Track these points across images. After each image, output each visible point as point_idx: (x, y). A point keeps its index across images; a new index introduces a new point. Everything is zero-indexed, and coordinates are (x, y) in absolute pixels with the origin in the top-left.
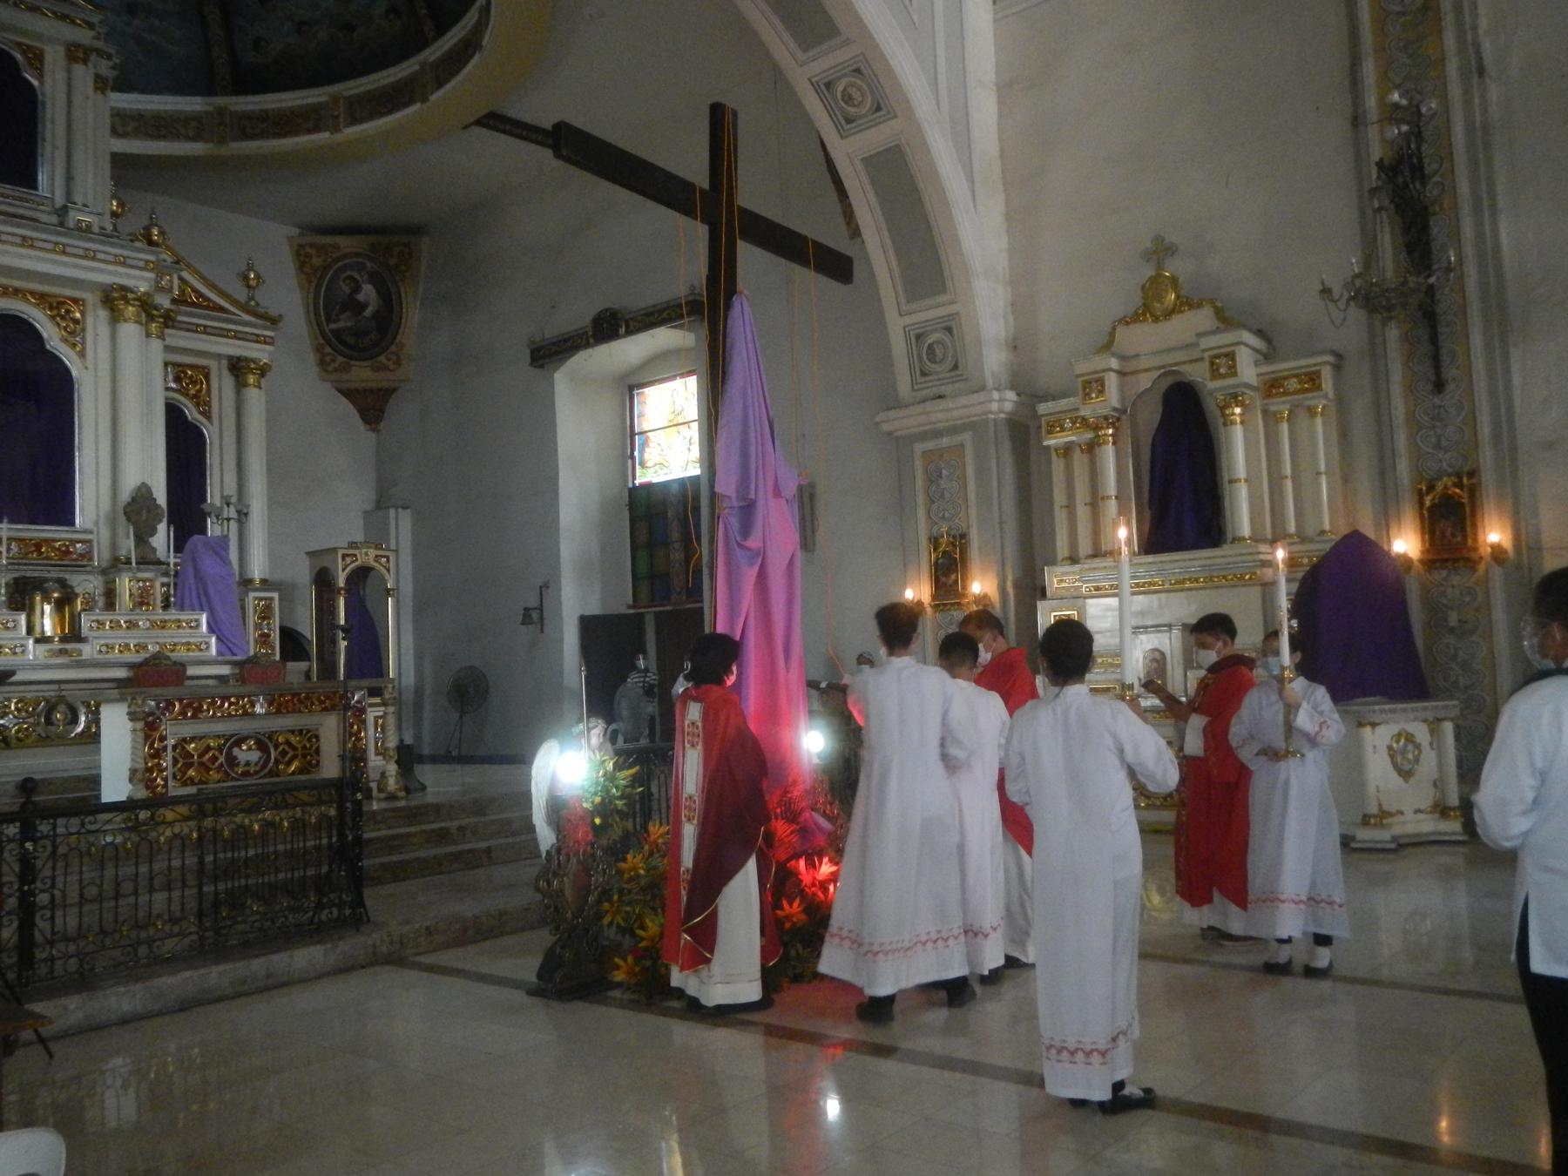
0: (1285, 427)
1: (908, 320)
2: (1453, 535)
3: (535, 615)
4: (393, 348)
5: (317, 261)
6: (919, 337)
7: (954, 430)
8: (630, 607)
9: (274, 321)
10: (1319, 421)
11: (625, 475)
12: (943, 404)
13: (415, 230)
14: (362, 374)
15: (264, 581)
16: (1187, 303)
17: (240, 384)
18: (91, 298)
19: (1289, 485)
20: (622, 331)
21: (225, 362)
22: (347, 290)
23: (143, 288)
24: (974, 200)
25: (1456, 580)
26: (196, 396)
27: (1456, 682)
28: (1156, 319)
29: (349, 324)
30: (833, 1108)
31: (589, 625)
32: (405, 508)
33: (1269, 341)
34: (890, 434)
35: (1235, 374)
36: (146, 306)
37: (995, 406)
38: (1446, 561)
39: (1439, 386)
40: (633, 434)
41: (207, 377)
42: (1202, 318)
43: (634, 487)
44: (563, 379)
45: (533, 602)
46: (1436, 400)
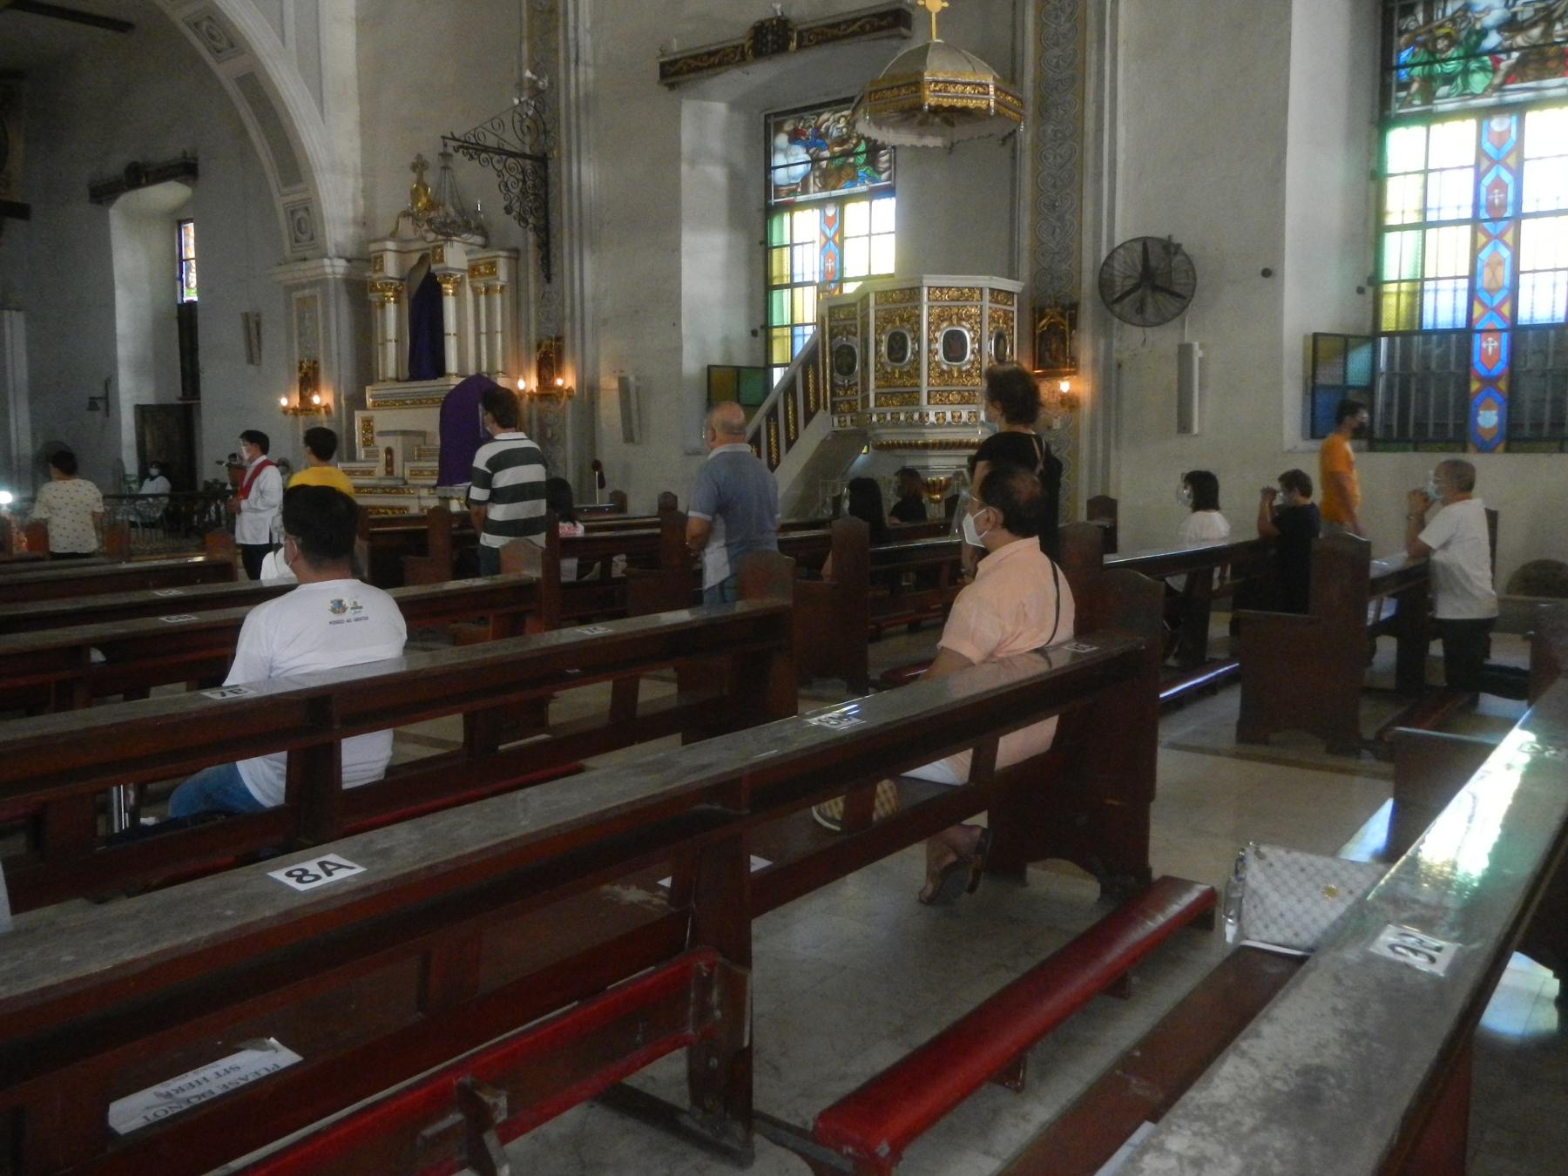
0: (483, 298)
3: (101, 404)
7: (313, 284)
10: (498, 297)
11: (175, 292)
12: (303, 266)
19: (483, 338)
24: (322, 112)
25: (552, 408)
31: (142, 412)
32: (18, 310)
33: (485, 234)
37: (328, 270)
39: (548, 278)
44: (116, 214)
45: (98, 391)
46: (548, 287)
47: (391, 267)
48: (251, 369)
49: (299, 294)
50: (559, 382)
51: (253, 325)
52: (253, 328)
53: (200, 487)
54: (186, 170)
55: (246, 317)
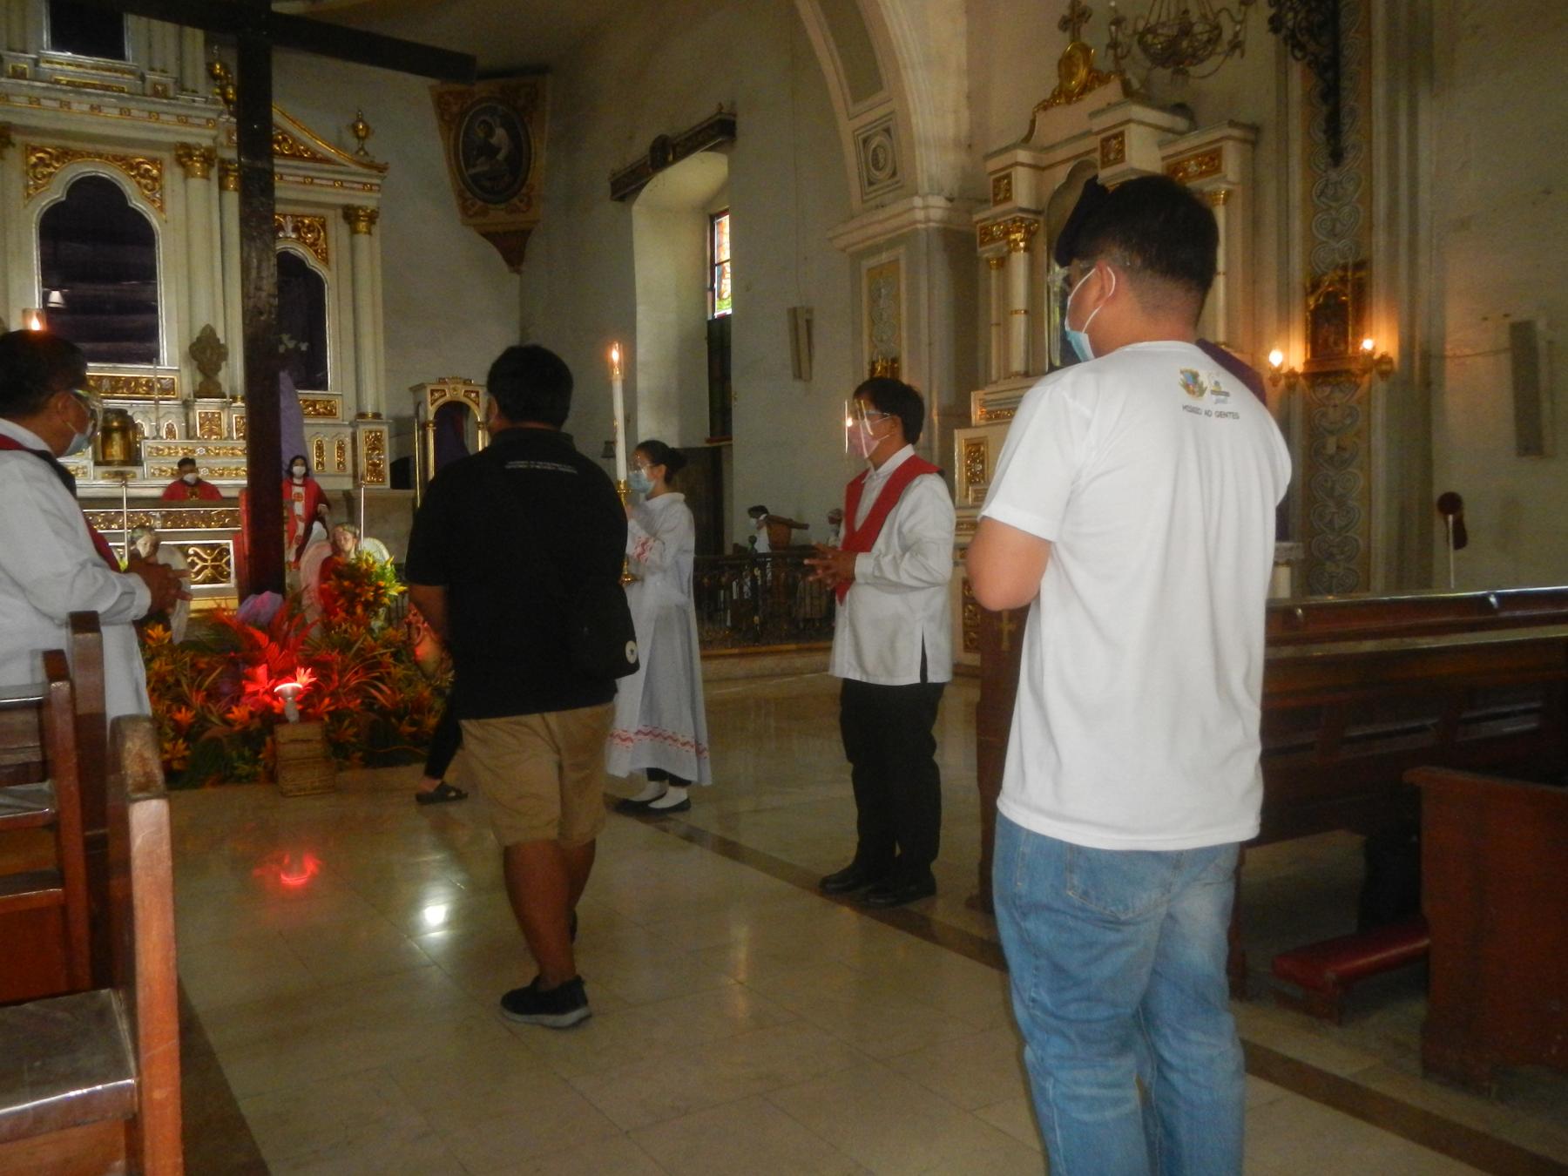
1: (857, 123)
2: (1336, 343)
4: (524, 190)
5: (455, 109)
6: (865, 141)
7: (892, 244)
8: (708, 441)
9: (382, 169)
11: (705, 307)
12: (881, 215)
13: (542, 69)
14: (499, 216)
15: (377, 416)
16: (1097, 79)
17: (354, 231)
18: (167, 157)
20: (671, 158)
21: (340, 212)
22: (481, 135)
23: (206, 143)
25: (1338, 397)
26: (313, 245)
27: (1331, 522)
28: (1069, 102)
29: (486, 168)
30: (435, 916)
34: (843, 250)
35: (1122, 160)
36: (208, 158)
37: (920, 215)
38: (1327, 374)
39: (1337, 157)
40: (713, 265)
41: (323, 226)
42: (1112, 91)
43: (714, 320)
44: (640, 211)
46: (1333, 175)
47: (1023, 192)
48: (799, 385)
49: (873, 262)
50: (1367, 345)
51: (802, 323)
52: (802, 327)
53: (729, 551)
54: (719, 132)
55: (794, 312)
